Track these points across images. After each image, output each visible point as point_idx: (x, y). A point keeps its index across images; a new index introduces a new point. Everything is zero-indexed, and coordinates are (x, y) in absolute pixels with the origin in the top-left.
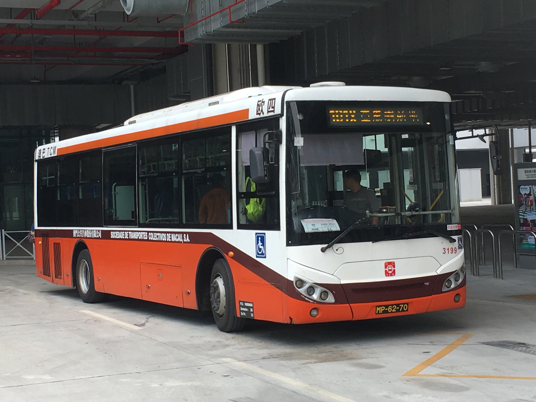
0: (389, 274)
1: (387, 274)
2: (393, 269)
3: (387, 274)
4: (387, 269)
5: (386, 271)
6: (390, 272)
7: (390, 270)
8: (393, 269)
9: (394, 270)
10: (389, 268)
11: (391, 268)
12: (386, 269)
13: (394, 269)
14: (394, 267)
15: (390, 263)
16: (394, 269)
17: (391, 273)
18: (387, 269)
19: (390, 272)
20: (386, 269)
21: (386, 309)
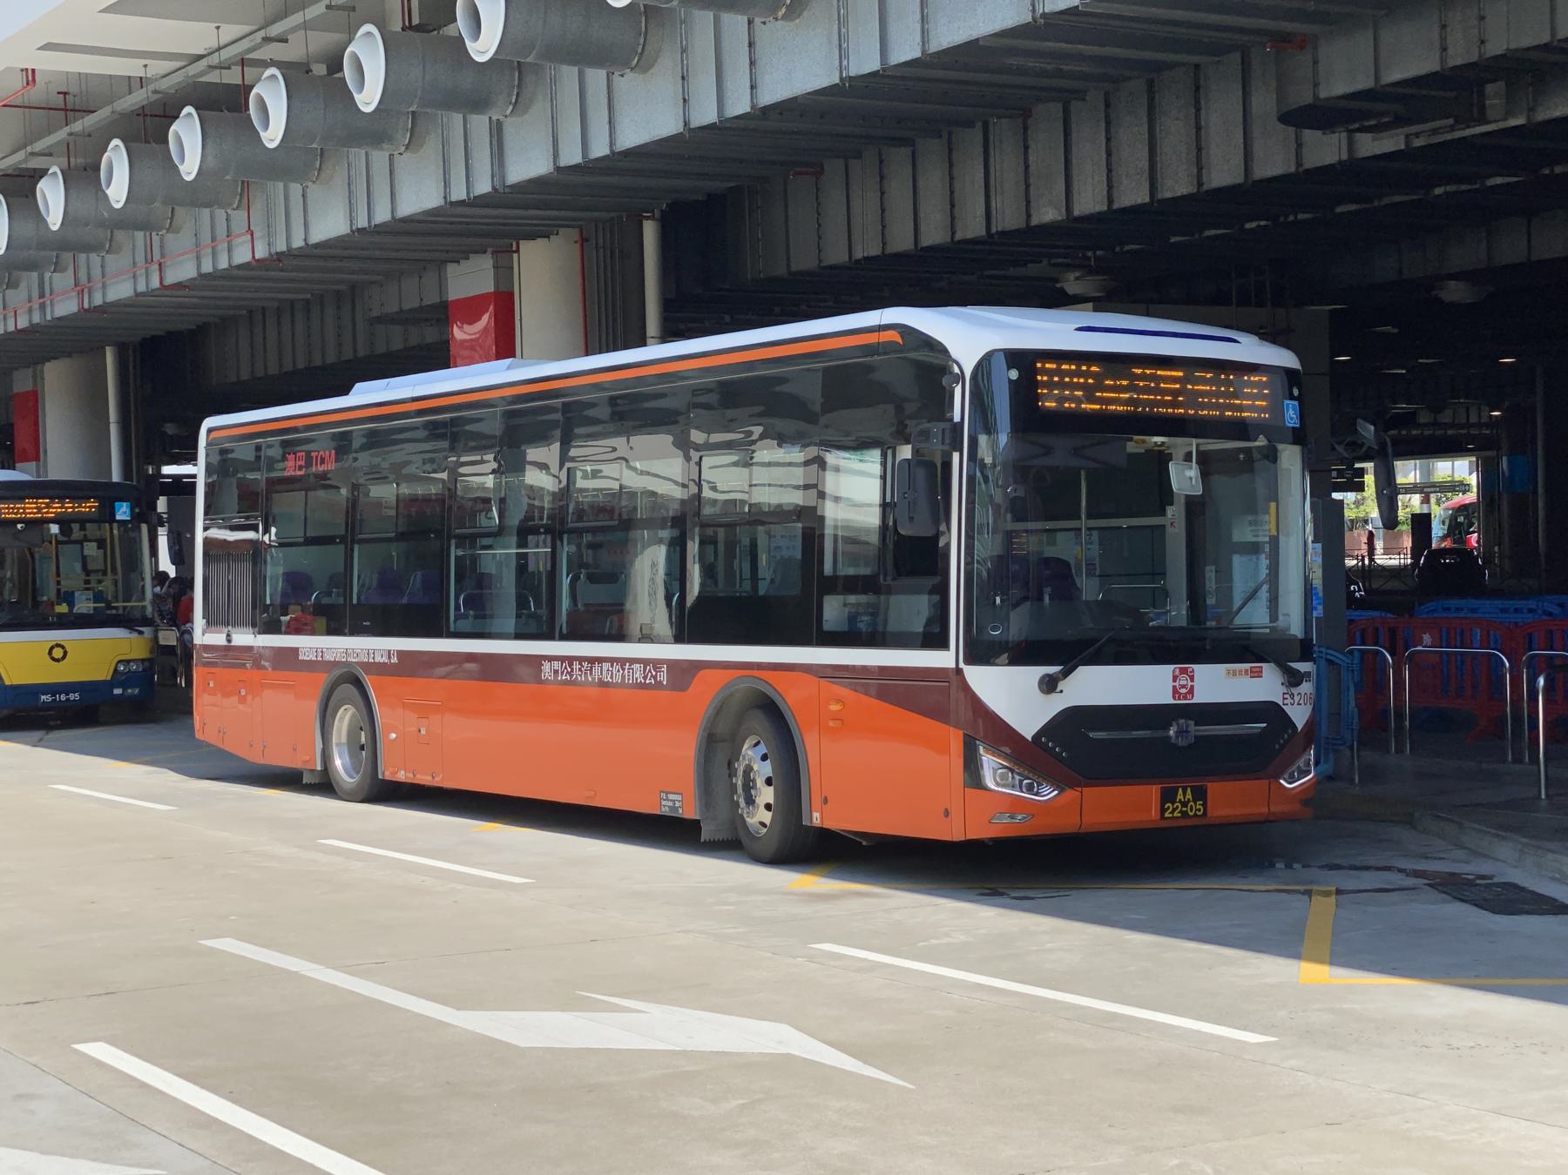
1: (1177, 695)
2: (1190, 684)
3: (1177, 695)
4: (1177, 684)
5: (1174, 687)
6: (1183, 691)
7: (1183, 686)
8: (1190, 684)
9: (1192, 687)
10: (1181, 683)
11: (1184, 683)
12: (1174, 684)
13: (1192, 684)
14: (1192, 680)
16: (1192, 684)
17: (1186, 694)
18: (1177, 684)
19: (1183, 691)
20: (1174, 684)
21: (1184, 809)
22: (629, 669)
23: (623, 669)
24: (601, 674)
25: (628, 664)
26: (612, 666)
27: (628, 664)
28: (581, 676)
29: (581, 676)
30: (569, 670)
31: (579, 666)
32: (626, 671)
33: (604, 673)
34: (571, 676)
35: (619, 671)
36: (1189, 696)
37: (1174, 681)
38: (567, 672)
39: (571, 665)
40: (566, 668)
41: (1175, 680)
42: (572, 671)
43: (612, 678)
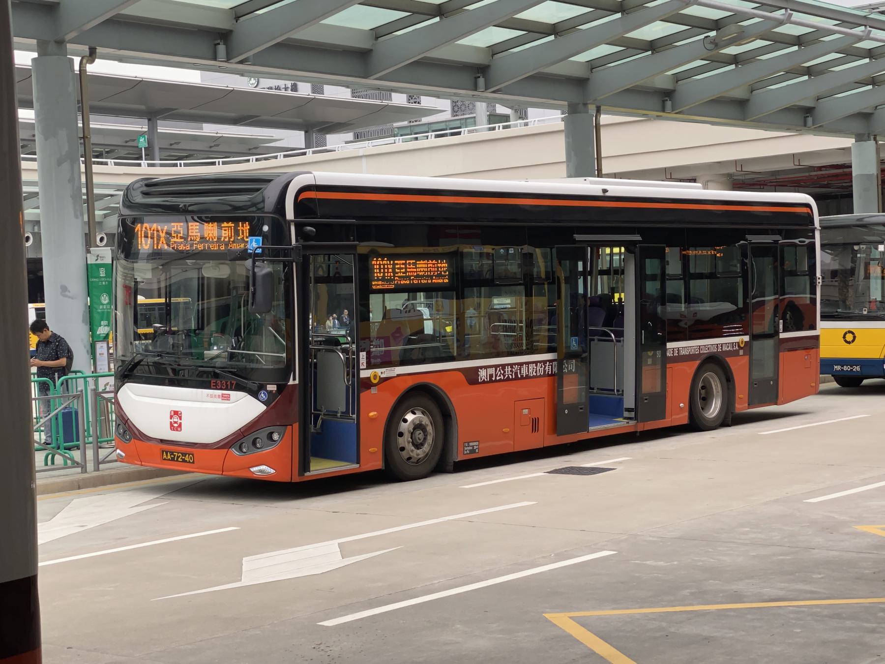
0: (174, 427)
1: (172, 428)
2: (179, 421)
4: (172, 420)
5: (171, 422)
6: (176, 425)
7: (176, 422)
8: (179, 421)
9: (181, 423)
13: (180, 421)
14: (181, 419)
15: (176, 413)
16: (180, 421)
17: (177, 427)
18: (172, 420)
19: (176, 425)
22: (549, 365)
23: (545, 367)
24: (528, 372)
25: (548, 363)
26: (536, 366)
27: (548, 363)
28: (512, 375)
29: (512, 375)
30: (502, 372)
31: (510, 369)
32: (547, 368)
33: (530, 371)
34: (504, 376)
35: (541, 367)
36: (179, 429)
37: (171, 418)
38: (501, 373)
39: (503, 369)
40: (500, 371)
41: (171, 417)
42: (505, 372)
43: (536, 372)
